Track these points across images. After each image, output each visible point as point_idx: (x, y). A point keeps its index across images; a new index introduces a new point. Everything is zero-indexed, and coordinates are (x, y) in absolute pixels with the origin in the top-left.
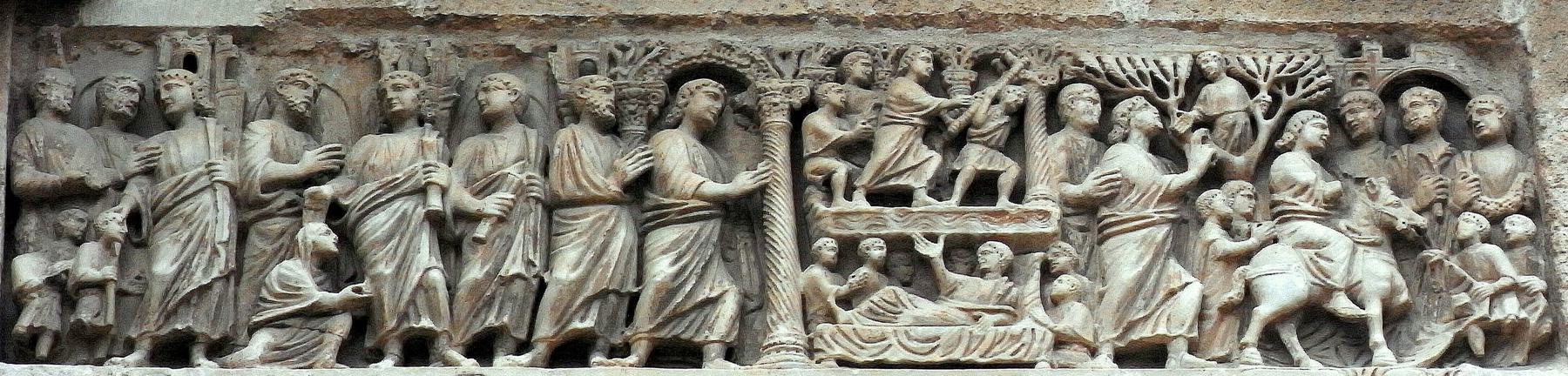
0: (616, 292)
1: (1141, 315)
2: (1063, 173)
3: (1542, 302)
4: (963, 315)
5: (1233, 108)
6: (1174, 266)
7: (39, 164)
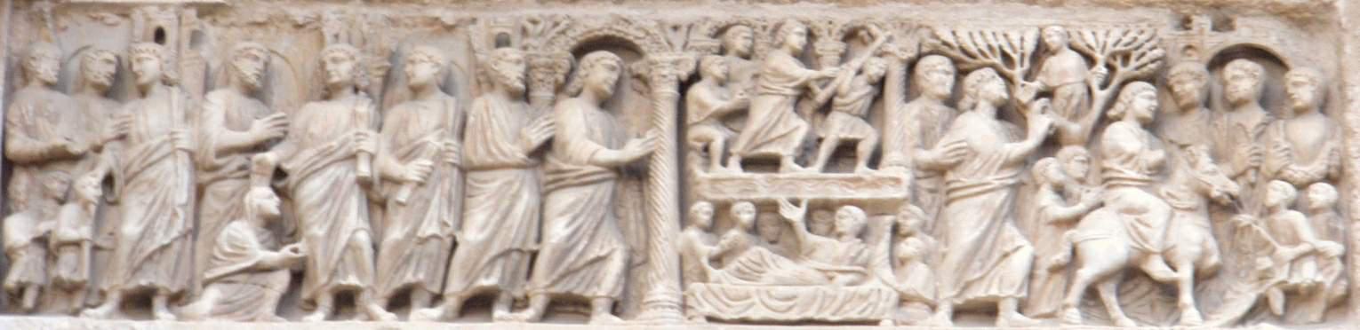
0: (519, 251)
1: (977, 275)
2: (917, 140)
3: (1338, 266)
4: (819, 276)
6: (1010, 229)
7: (30, 131)
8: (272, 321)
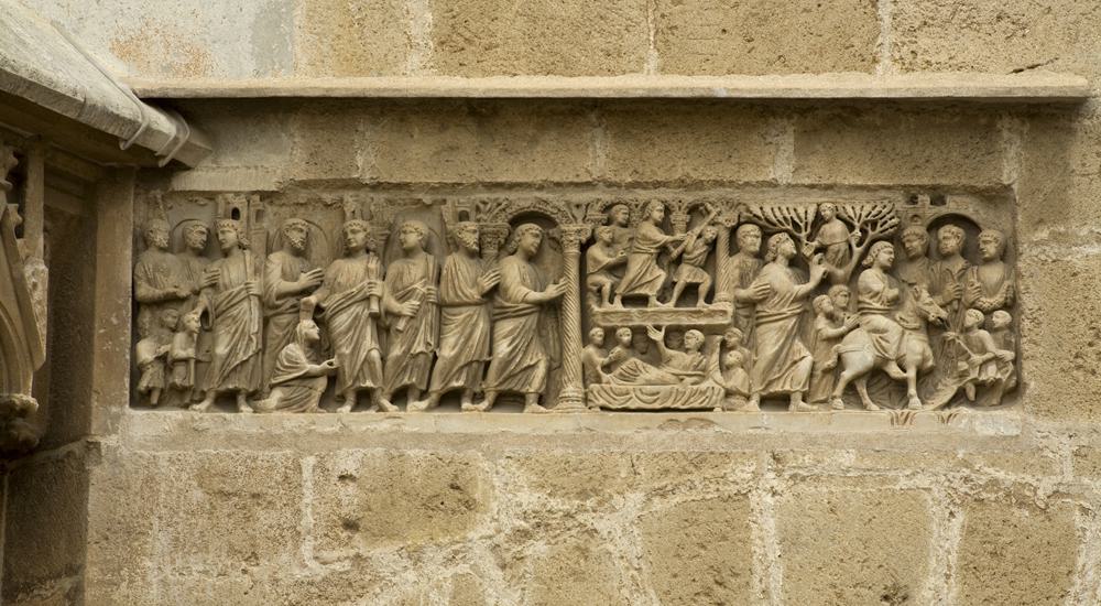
0: (477, 361)
2: (737, 283)
3: (1011, 367)
4: (674, 378)
5: (838, 241)
6: (798, 344)
7: (149, 281)
8: (316, 412)
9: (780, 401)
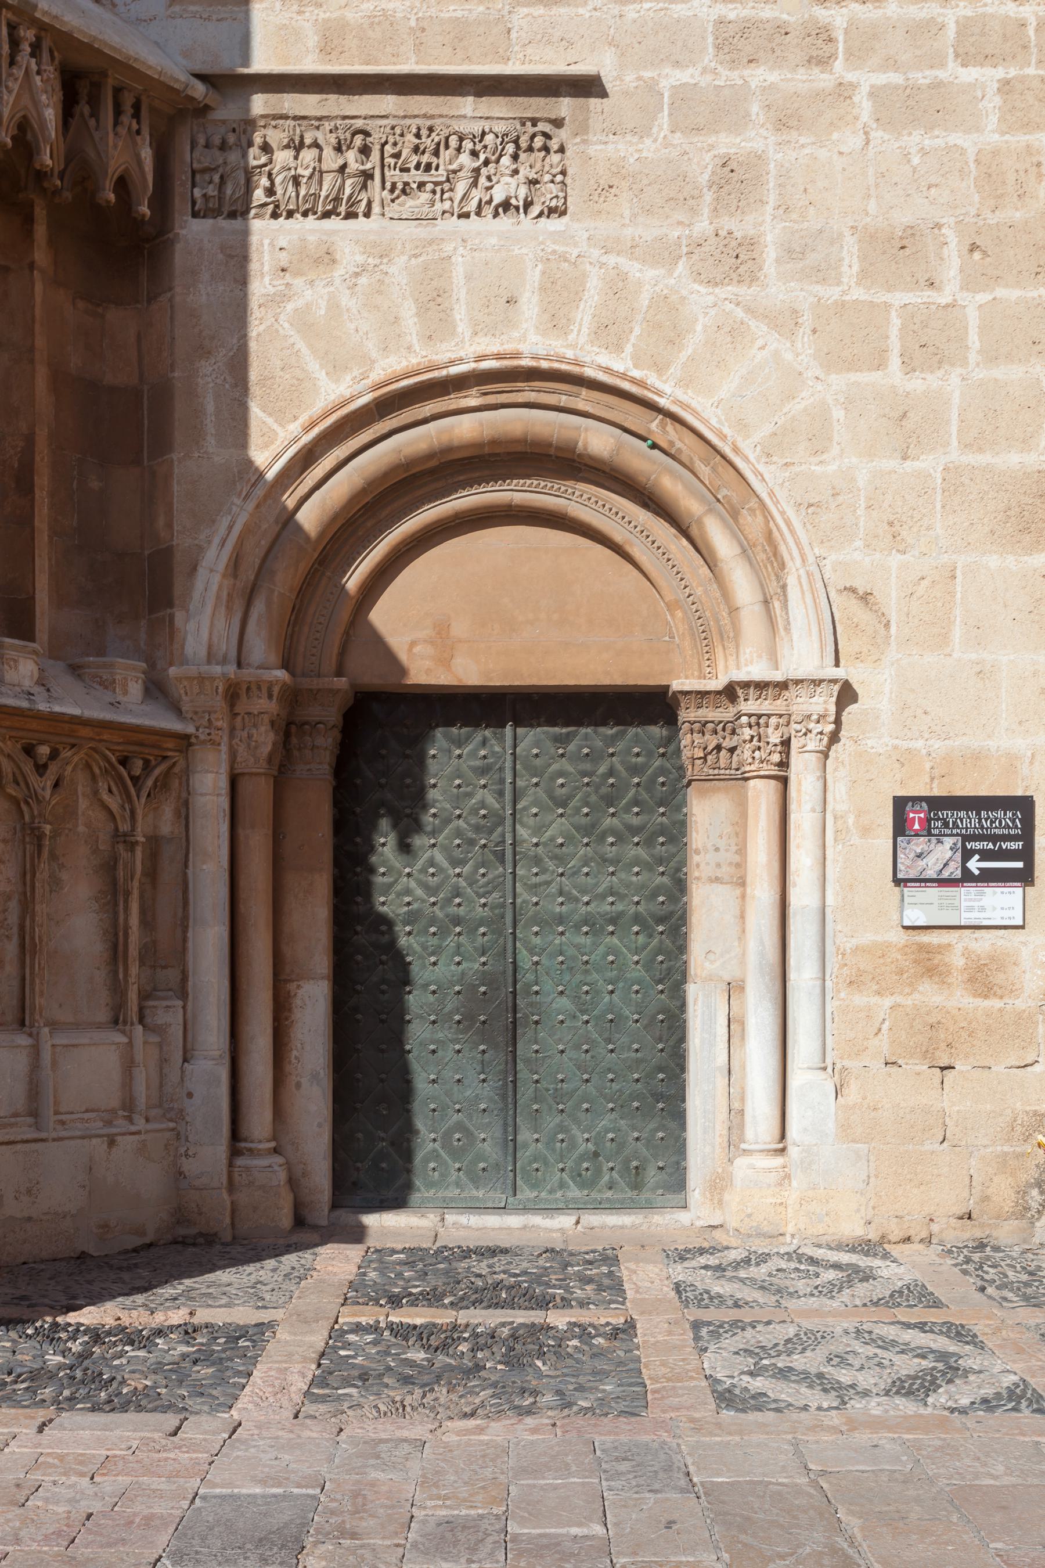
9: (466, 215)
